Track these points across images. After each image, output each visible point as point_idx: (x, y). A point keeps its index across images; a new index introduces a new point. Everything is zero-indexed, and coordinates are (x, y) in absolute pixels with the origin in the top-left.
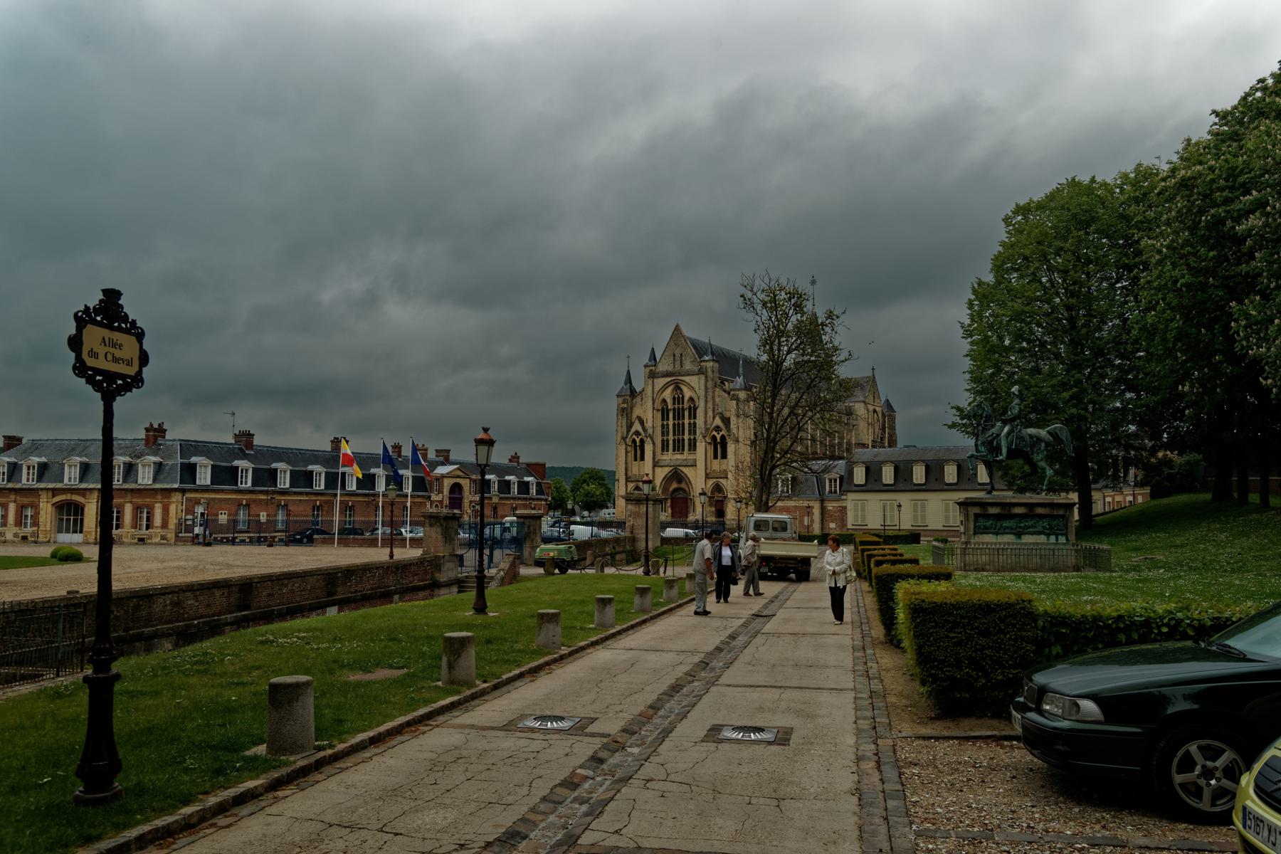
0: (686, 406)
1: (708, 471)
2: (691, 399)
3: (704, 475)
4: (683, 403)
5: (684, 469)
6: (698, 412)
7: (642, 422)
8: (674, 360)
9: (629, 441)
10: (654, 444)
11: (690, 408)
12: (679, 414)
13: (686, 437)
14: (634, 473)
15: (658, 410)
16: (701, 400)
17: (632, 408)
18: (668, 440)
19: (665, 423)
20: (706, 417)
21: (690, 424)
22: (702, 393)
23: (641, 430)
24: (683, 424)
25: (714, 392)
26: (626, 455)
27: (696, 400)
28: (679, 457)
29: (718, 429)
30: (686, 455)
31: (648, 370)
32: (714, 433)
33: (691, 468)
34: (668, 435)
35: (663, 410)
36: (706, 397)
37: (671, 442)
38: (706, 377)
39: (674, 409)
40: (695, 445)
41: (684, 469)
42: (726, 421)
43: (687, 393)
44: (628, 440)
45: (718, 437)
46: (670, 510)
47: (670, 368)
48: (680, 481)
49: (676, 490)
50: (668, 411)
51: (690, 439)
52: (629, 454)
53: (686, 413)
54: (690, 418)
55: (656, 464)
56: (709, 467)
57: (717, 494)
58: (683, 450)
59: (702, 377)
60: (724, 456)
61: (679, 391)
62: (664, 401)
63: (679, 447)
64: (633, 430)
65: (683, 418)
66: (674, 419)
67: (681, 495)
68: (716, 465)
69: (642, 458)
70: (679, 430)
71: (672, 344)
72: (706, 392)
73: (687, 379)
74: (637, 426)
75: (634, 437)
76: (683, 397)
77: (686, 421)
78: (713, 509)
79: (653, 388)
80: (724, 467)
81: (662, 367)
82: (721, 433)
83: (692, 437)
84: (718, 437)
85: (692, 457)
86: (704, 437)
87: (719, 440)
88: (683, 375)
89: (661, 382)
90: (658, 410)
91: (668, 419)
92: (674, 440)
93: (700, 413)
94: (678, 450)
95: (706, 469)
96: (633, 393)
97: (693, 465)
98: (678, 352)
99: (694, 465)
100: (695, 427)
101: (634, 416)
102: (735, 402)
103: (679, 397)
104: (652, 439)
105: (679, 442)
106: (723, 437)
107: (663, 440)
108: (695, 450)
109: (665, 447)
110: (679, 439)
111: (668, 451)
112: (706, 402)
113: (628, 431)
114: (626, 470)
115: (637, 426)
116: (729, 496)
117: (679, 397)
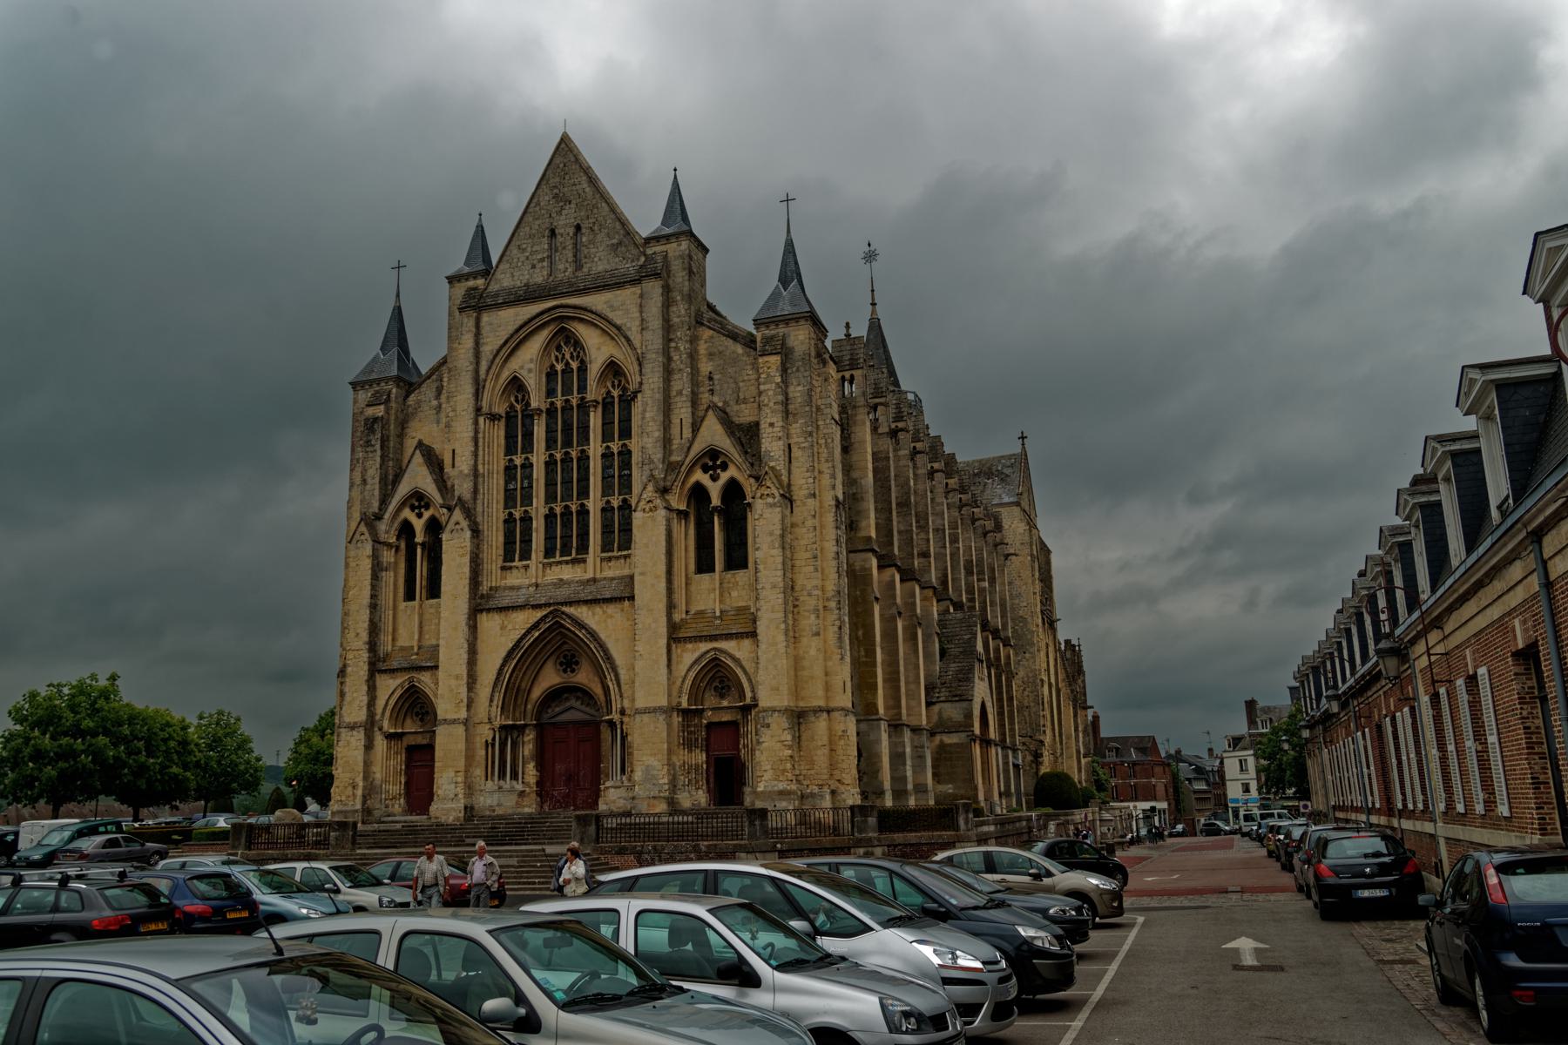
0: (594, 392)
1: (677, 617)
2: (613, 369)
3: (663, 630)
4: (582, 388)
5: (583, 613)
6: (637, 409)
7: (434, 462)
8: (553, 249)
9: (385, 528)
10: (476, 532)
11: (607, 405)
12: (567, 428)
13: (594, 503)
14: (403, 641)
15: (493, 417)
16: (647, 368)
17: (403, 425)
18: (527, 520)
19: (518, 461)
20: (666, 426)
21: (607, 455)
22: (652, 341)
23: (429, 487)
24: (584, 458)
25: (694, 340)
26: (375, 577)
27: (630, 367)
28: (568, 573)
29: (713, 460)
30: (594, 566)
31: (461, 289)
32: (699, 476)
33: (611, 609)
34: (527, 499)
35: (510, 417)
36: (666, 353)
37: (538, 525)
38: (667, 289)
39: (551, 412)
40: (627, 529)
41: (583, 613)
42: (748, 436)
43: (598, 349)
44: (382, 527)
45: (715, 491)
46: (531, 773)
47: (539, 277)
48: (569, 664)
49: (554, 695)
50: (529, 416)
51: (607, 510)
52: (388, 577)
53: (595, 420)
54: (607, 436)
55: (481, 604)
56: (680, 598)
57: (711, 700)
58: (583, 547)
59: (654, 288)
60: (737, 558)
61: (567, 351)
62: (516, 384)
63: (567, 538)
64: (403, 489)
65: (584, 437)
66: (550, 443)
67: (574, 712)
68: (708, 594)
69: (434, 590)
70: (567, 482)
71: (545, 198)
72: (667, 340)
73: (596, 301)
74: (418, 477)
75: (407, 513)
76: (583, 369)
77: (595, 448)
78: (700, 757)
79: (477, 344)
80: (738, 598)
81: (505, 280)
82: (724, 477)
83: (616, 503)
84: (715, 491)
85: (615, 570)
86: (664, 491)
87: (716, 501)
88: (585, 291)
89: (502, 322)
90: (493, 417)
91: (528, 447)
92: (550, 518)
93: (645, 413)
94: (566, 550)
95: (671, 607)
96: (408, 381)
97: (625, 595)
98: (564, 224)
99: (625, 595)
100: (626, 463)
101: (410, 444)
102: (775, 360)
103: (567, 370)
104: (469, 514)
105: (567, 524)
106: (733, 491)
107: (509, 521)
108: (626, 543)
109: (516, 545)
110: (567, 512)
111: (526, 555)
112: (668, 373)
113: (384, 502)
114: (374, 629)
115: (418, 477)
116: (764, 702)
117: (567, 370)
